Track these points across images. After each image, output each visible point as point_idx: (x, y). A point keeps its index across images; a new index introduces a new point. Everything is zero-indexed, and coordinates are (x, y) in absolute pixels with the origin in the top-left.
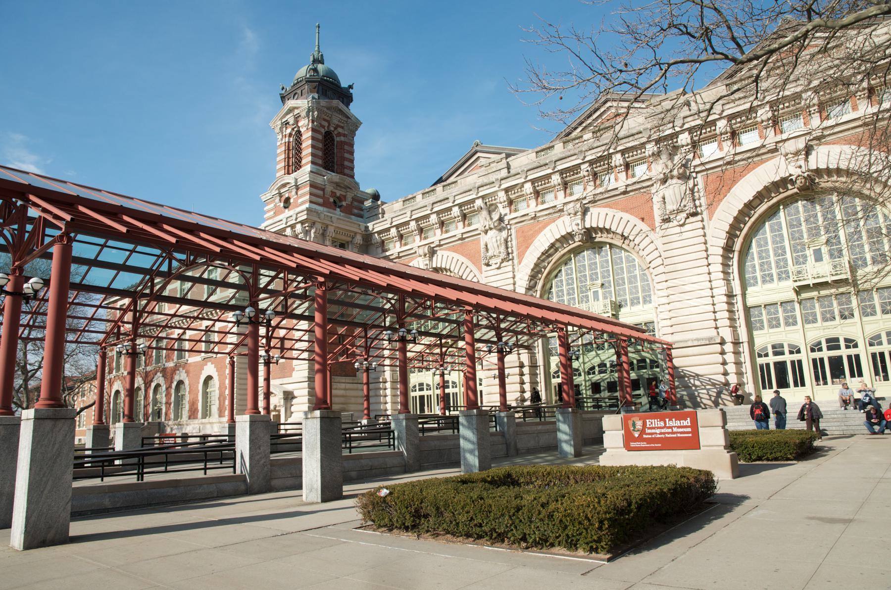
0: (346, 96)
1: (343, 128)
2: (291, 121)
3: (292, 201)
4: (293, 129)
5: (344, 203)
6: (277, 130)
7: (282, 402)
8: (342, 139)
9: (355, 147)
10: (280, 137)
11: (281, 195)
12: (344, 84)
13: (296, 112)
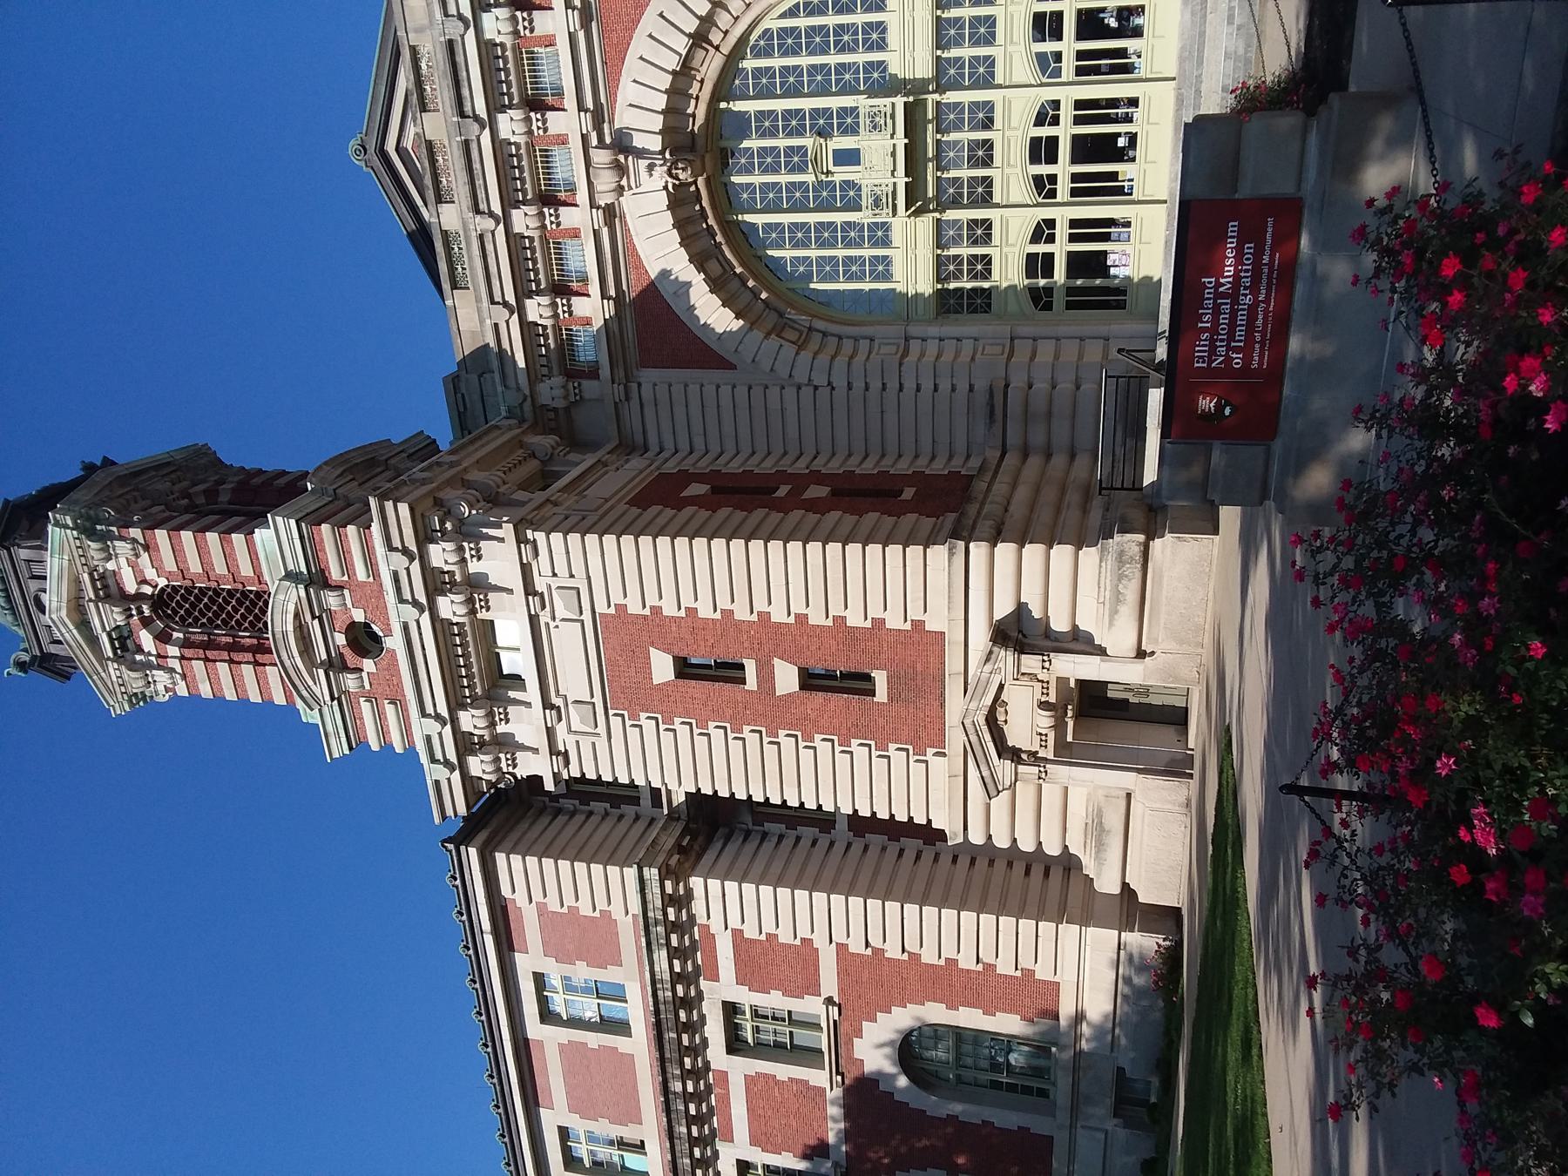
2: (116, 616)
3: (359, 616)
4: (146, 623)
6: (135, 682)
7: (1031, 663)
9: (270, 466)
10: (160, 675)
11: (336, 665)
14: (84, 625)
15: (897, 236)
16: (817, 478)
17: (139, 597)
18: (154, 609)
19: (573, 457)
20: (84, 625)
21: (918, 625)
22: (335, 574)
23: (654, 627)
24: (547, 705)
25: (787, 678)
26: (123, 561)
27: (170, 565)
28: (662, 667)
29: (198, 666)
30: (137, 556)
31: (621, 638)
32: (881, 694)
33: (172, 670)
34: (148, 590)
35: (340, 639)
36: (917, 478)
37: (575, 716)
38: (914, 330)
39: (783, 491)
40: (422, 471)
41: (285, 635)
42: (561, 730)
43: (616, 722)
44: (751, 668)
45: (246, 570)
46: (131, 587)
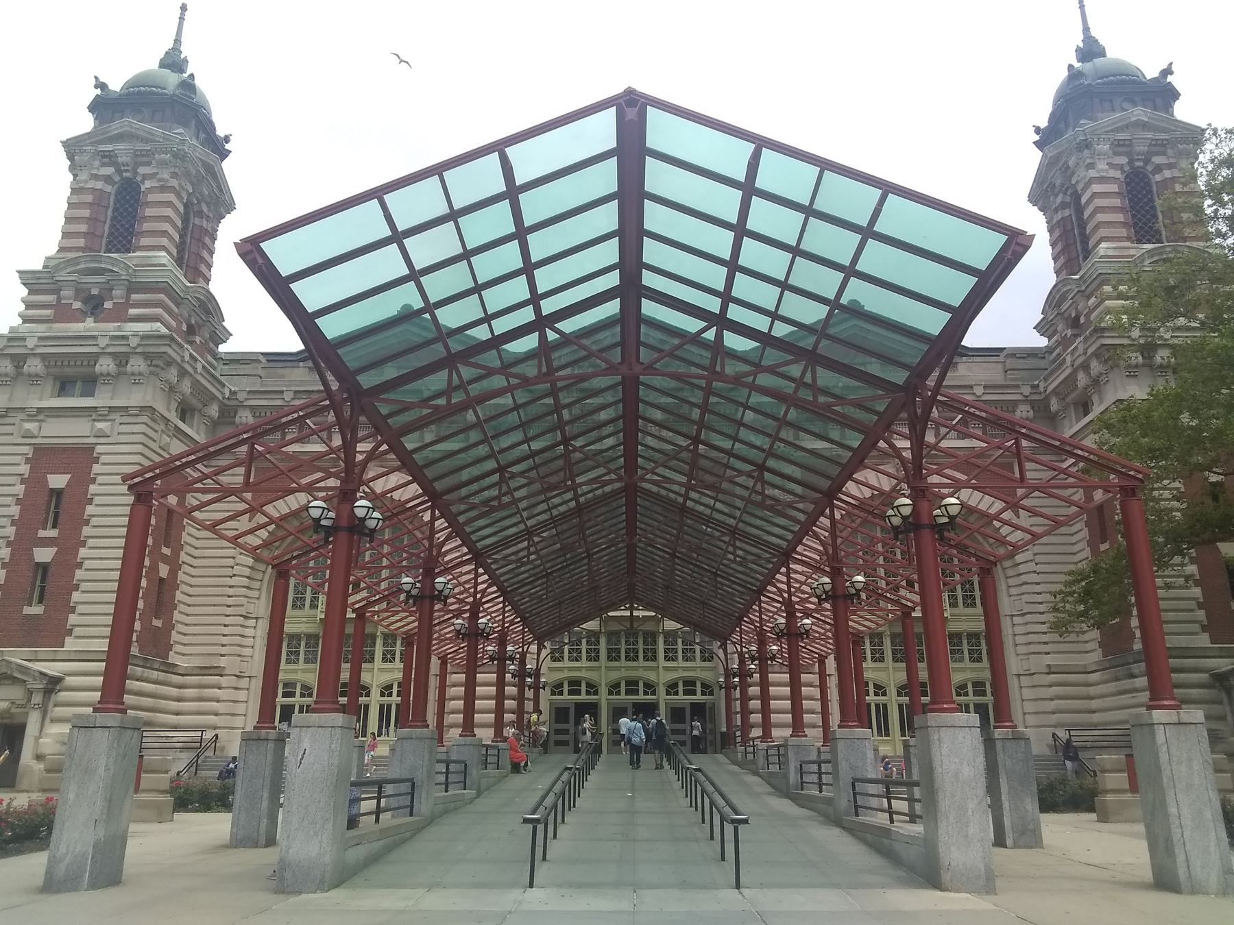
0: (224, 154)
1: (208, 204)
3: (108, 305)
5: (198, 339)
8: (205, 224)
12: (221, 132)
13: (140, 146)
14: (120, 137)
15: (313, 612)
16: (174, 572)
17: (136, 173)
18: (127, 178)
19: (203, 427)
20: (120, 137)
21: (69, 633)
22: (134, 297)
23: (83, 479)
24: (40, 410)
25: (44, 555)
26: (155, 170)
27: (152, 197)
28: (58, 481)
29: (89, 198)
30: (159, 180)
31: (80, 458)
32: (28, 610)
33: (86, 182)
34: (139, 178)
35: (95, 292)
36: (169, 626)
37: (31, 426)
38: (260, 621)
39: (166, 551)
40: (191, 354)
41: (100, 262)
42: (21, 416)
43: (25, 449)
44: (53, 533)
45: (145, 241)
46: (142, 170)
